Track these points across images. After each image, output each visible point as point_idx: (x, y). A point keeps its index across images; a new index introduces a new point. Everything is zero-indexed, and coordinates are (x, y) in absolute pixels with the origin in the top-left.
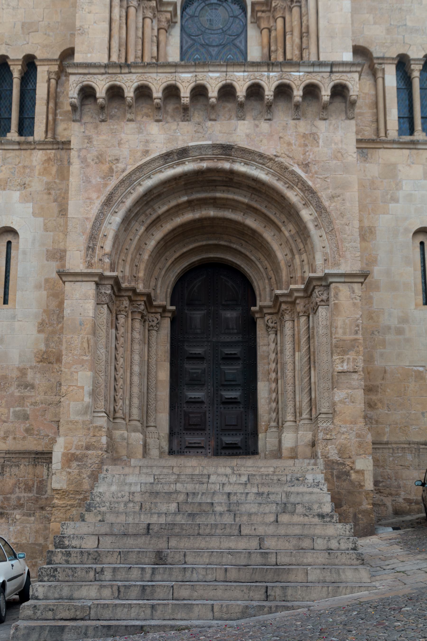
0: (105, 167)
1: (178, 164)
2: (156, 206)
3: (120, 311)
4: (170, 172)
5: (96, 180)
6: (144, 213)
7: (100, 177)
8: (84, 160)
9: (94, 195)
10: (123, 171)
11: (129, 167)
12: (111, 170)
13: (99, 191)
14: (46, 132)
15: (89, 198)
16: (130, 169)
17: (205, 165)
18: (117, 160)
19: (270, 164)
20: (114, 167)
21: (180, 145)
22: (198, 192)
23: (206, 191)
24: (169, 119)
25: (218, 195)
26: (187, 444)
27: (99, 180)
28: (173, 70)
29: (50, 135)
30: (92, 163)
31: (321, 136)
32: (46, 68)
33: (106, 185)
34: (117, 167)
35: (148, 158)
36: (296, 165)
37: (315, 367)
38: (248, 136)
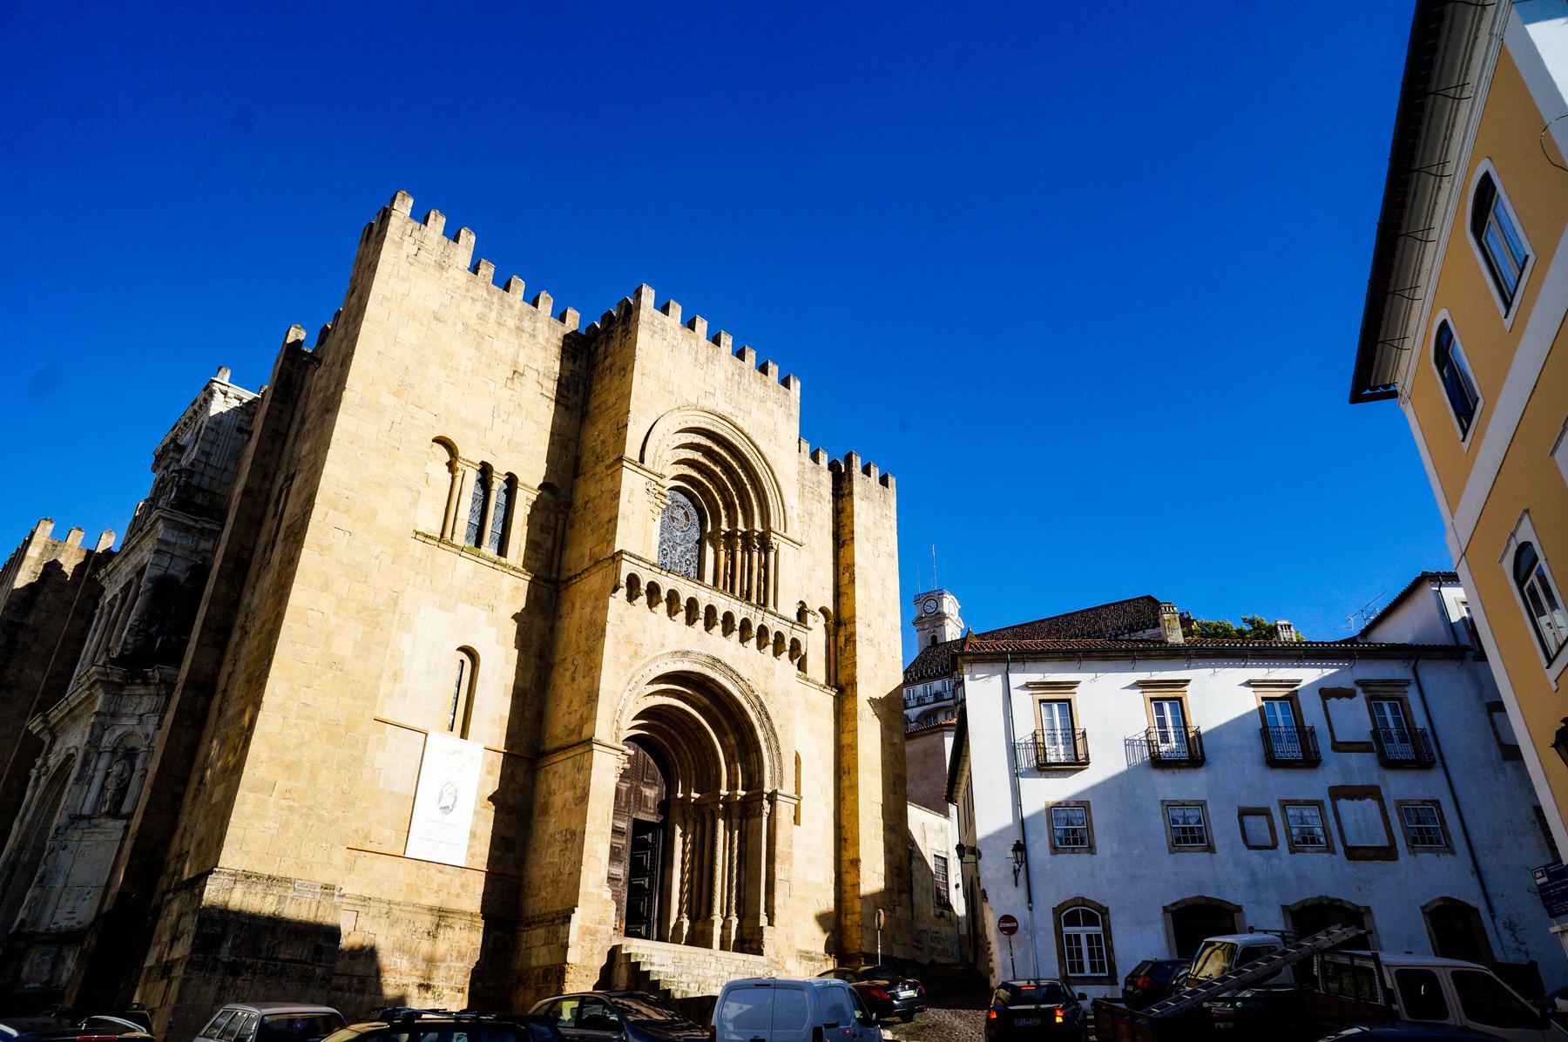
0: (632, 648)
5: (624, 658)
8: (616, 636)
9: (622, 672)
10: (646, 656)
11: (649, 654)
15: (617, 673)
17: (697, 668)
18: (641, 645)
19: (741, 683)
20: (638, 651)
21: (687, 648)
27: (627, 658)
28: (696, 586)
30: (623, 641)
31: (776, 673)
32: (526, 493)
33: (631, 665)
37: (746, 868)
38: (731, 655)
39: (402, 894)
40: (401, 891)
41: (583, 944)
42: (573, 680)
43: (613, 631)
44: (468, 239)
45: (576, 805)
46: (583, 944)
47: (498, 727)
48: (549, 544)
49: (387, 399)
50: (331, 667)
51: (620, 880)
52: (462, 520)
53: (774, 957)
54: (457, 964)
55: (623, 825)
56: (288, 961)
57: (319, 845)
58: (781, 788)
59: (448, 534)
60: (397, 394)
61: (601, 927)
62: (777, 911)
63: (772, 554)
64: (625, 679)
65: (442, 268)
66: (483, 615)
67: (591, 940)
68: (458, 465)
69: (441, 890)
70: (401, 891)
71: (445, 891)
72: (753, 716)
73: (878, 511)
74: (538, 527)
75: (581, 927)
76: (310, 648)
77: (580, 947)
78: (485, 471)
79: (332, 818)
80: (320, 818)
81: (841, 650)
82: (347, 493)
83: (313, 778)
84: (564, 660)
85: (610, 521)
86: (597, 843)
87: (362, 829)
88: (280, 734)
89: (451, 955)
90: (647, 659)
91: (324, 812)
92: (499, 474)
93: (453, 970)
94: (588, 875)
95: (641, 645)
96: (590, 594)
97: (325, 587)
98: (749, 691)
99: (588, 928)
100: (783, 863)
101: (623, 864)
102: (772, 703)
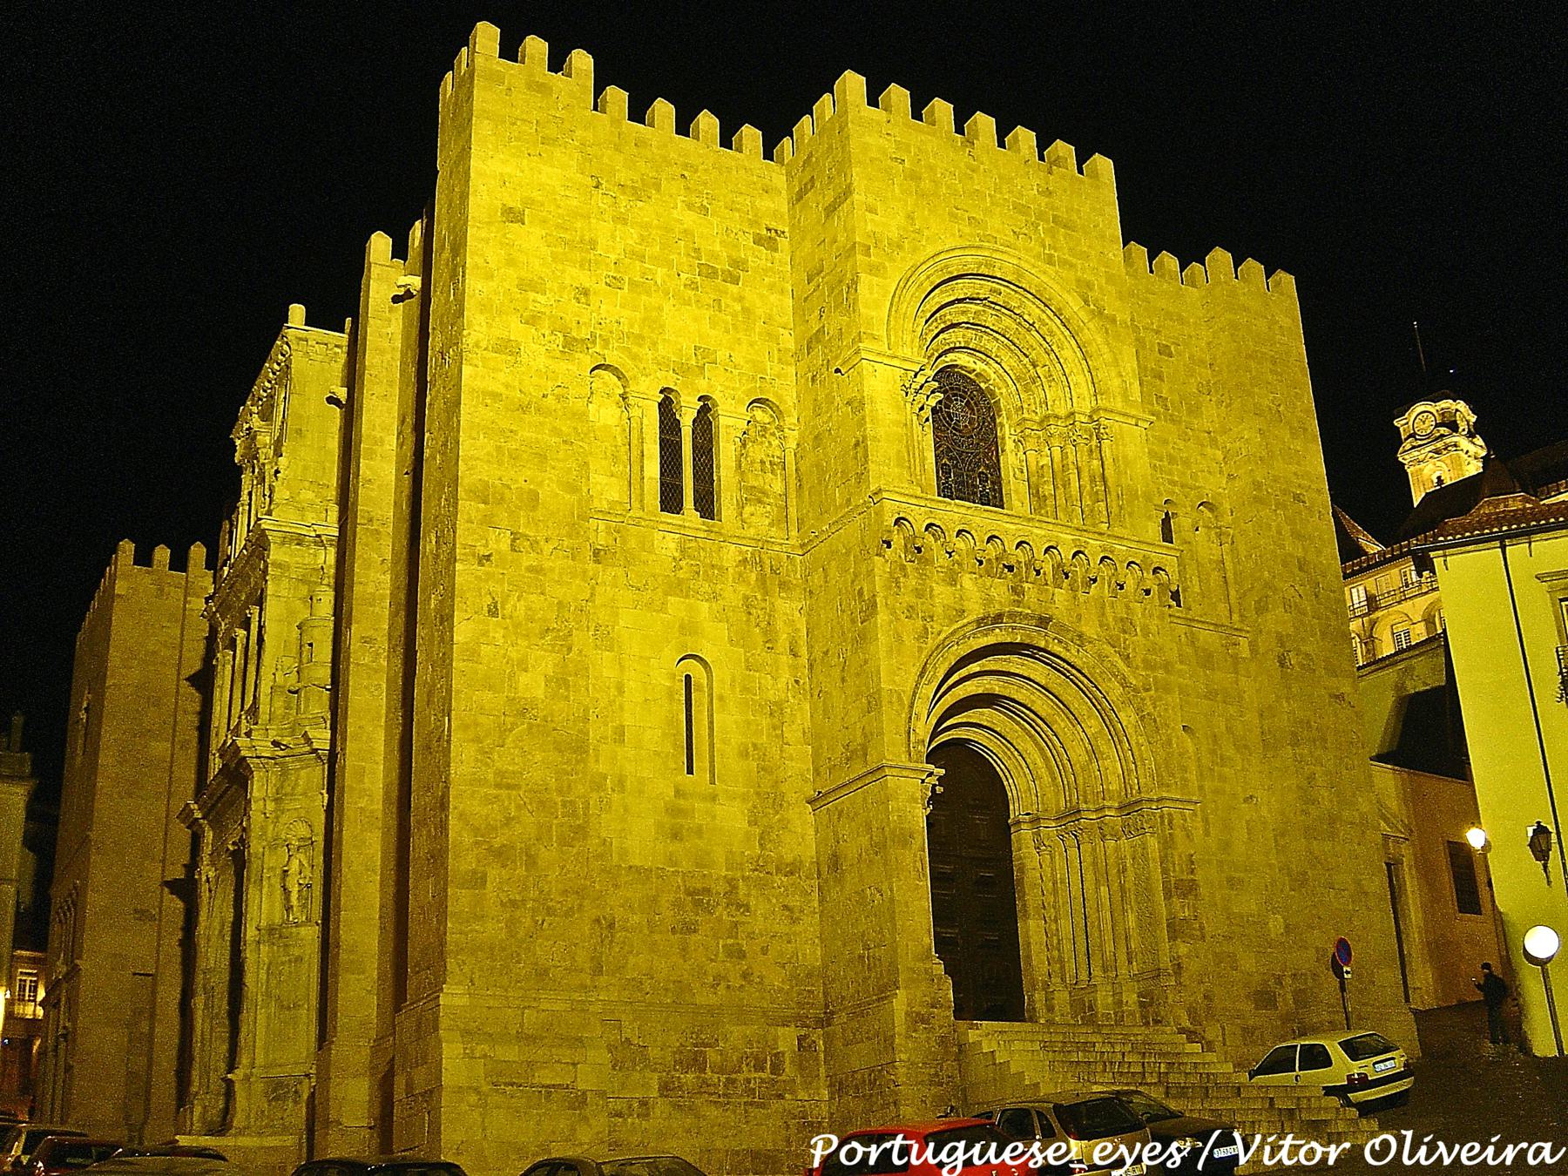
5: (909, 640)
16: (947, 631)
19: (1088, 647)
30: (903, 617)
32: (731, 422)
34: (932, 627)
35: (965, 621)
40: (667, 990)
42: (843, 680)
44: (582, 61)
45: (876, 854)
48: (778, 487)
49: (516, 329)
52: (651, 478)
53: (1187, 1024)
55: (948, 868)
59: (636, 505)
60: (532, 320)
62: (1185, 962)
64: (916, 670)
68: (631, 401)
69: (718, 985)
71: (723, 984)
72: (1115, 691)
74: (758, 466)
76: (490, 695)
79: (564, 909)
80: (550, 911)
83: (531, 862)
84: (826, 653)
85: (857, 444)
87: (604, 918)
89: (747, 1065)
90: (943, 636)
95: (932, 617)
96: (848, 553)
97: (493, 612)
98: (1101, 657)
99: (918, 1014)
102: (1137, 669)
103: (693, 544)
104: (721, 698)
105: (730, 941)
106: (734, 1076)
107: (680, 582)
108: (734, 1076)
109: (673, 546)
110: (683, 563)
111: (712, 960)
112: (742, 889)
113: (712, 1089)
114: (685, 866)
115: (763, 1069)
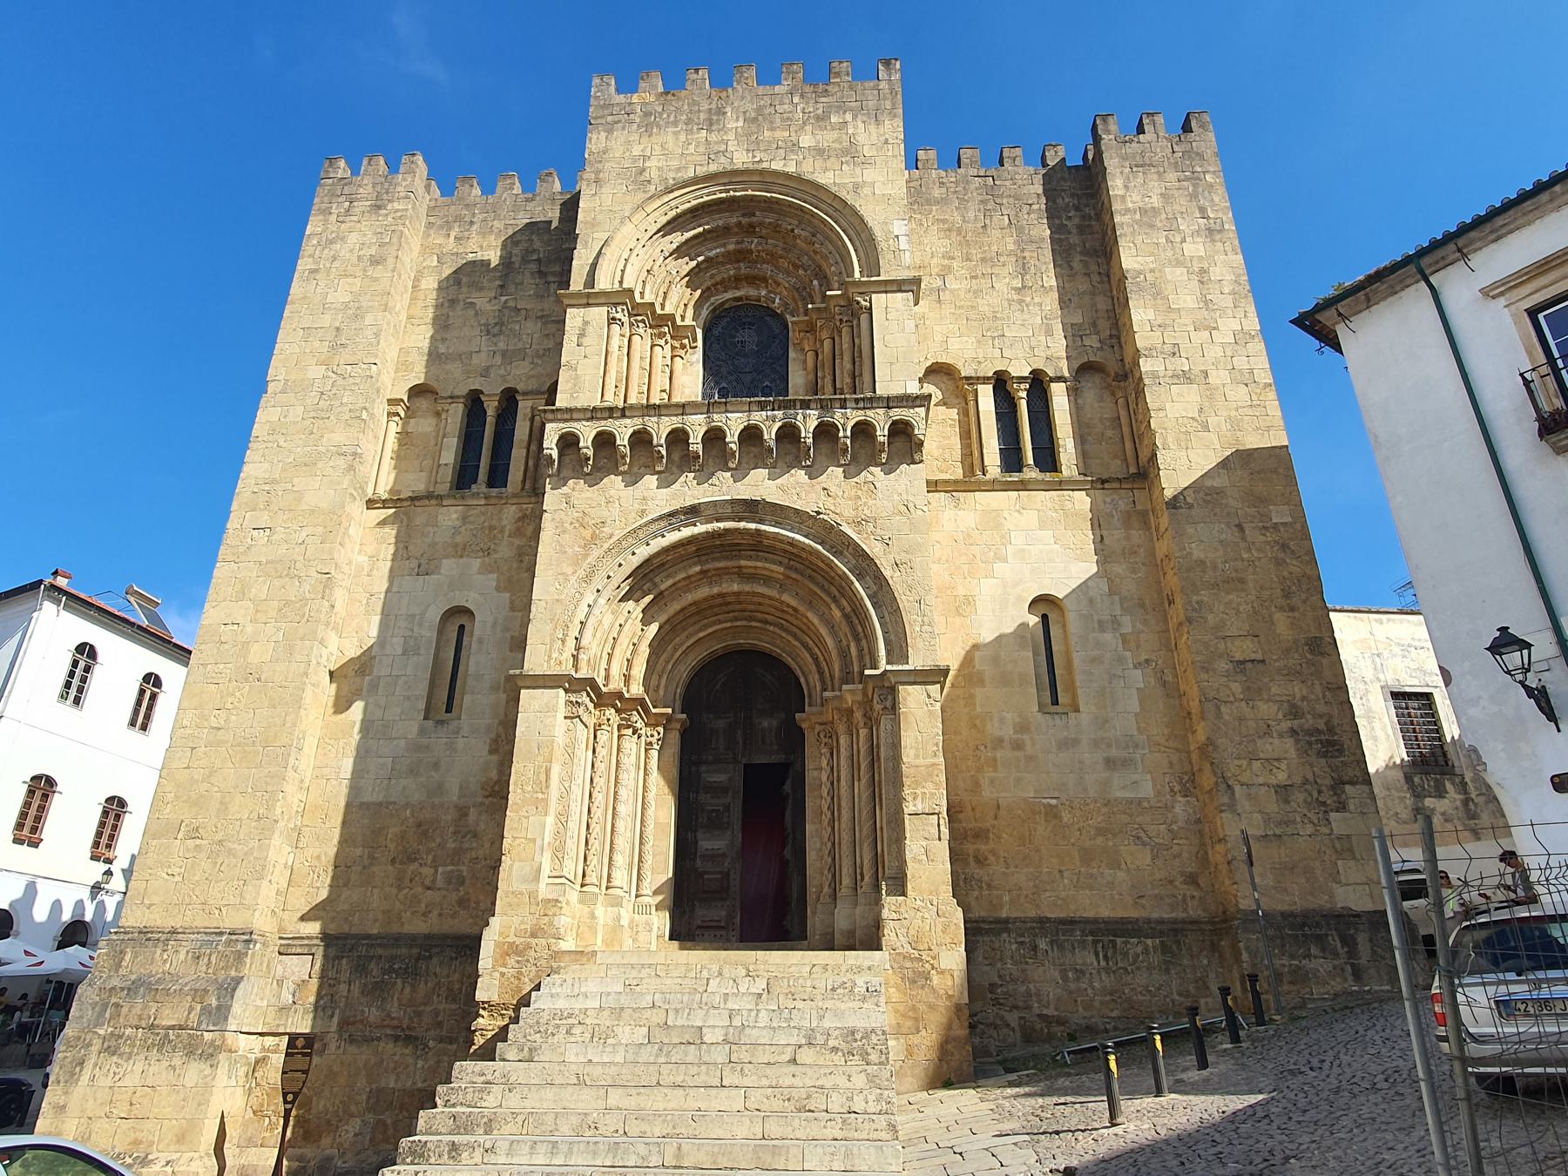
0: (587, 534)
1: (686, 526)
2: (657, 580)
3: (600, 725)
4: (673, 537)
6: (641, 588)
7: (579, 547)
9: (569, 571)
12: (594, 536)
13: (576, 563)
14: (524, 481)
16: (618, 534)
22: (717, 559)
23: (727, 558)
24: (674, 469)
25: (743, 563)
26: (699, 923)
29: (528, 486)
32: (530, 403)
33: (586, 556)
35: (645, 520)
36: (844, 524)
39: (378, 924)
41: (503, 970)
43: (553, 519)
46: (503, 970)
47: (504, 692)
50: (247, 680)
51: (724, 855)
52: (446, 465)
54: (448, 1006)
56: (172, 1028)
57: (230, 884)
58: (905, 659)
61: (534, 941)
63: (864, 317)
65: (379, 207)
66: (476, 563)
67: (518, 962)
69: (430, 912)
70: (376, 920)
71: (435, 912)
73: (1172, 176)
75: (498, 945)
76: (221, 666)
77: (497, 975)
78: (474, 402)
79: (246, 849)
80: (231, 853)
81: (1135, 414)
82: (267, 487)
86: (528, 818)
88: (188, 768)
89: (438, 996)
90: (615, 539)
91: (236, 846)
92: (489, 395)
93: (442, 1014)
94: (511, 867)
97: (241, 595)
99: (511, 944)
100: (917, 784)
101: (729, 833)
103: (475, 511)
104: (480, 641)
105: (449, 868)
106: (422, 1008)
107: (456, 545)
108: (422, 1008)
109: (454, 516)
110: (462, 529)
111: (429, 888)
112: (472, 816)
113: (395, 1022)
114: (417, 797)
115: (454, 1000)
